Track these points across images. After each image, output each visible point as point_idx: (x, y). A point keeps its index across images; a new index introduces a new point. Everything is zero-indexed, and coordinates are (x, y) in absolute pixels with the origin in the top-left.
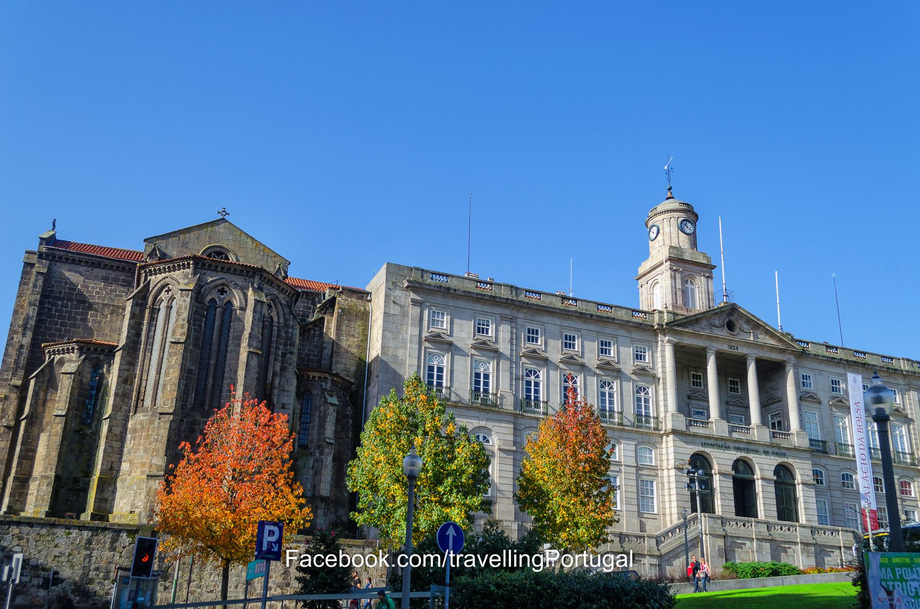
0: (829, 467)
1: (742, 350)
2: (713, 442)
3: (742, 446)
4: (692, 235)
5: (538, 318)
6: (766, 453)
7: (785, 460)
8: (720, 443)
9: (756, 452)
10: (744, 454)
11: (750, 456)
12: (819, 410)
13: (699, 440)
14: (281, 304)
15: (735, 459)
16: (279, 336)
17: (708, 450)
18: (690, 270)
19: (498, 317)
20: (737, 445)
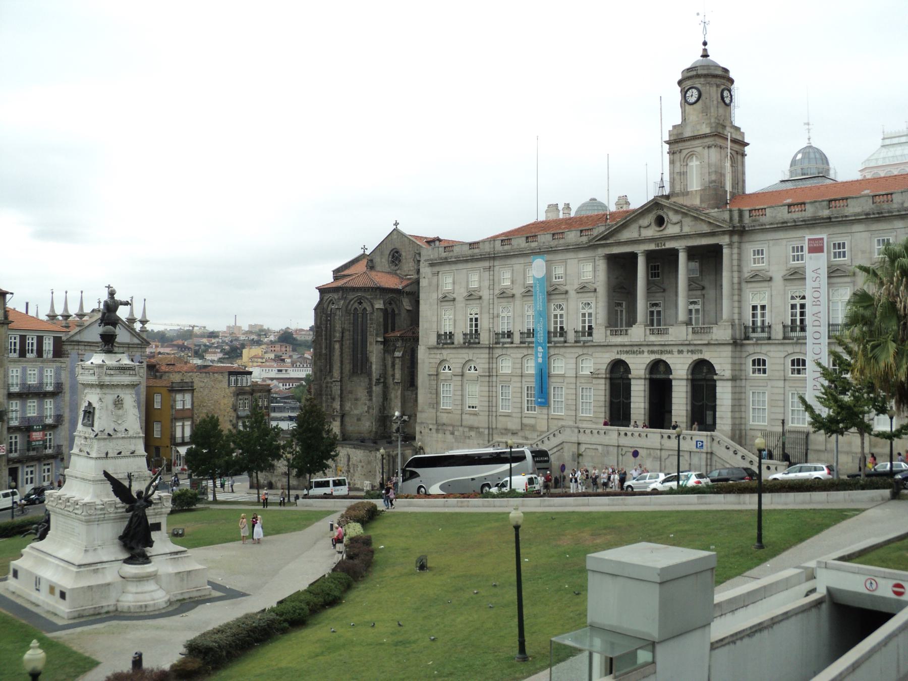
0: (771, 354)
1: (669, 245)
2: (628, 349)
3: (655, 348)
4: (700, 101)
5: (509, 261)
6: (680, 352)
7: (700, 356)
8: (635, 349)
9: (670, 352)
10: (657, 356)
11: (664, 357)
12: (769, 289)
13: (615, 350)
14: (367, 299)
15: (648, 361)
16: (371, 319)
17: (623, 357)
18: (691, 147)
19: (482, 270)
20: (651, 348)
